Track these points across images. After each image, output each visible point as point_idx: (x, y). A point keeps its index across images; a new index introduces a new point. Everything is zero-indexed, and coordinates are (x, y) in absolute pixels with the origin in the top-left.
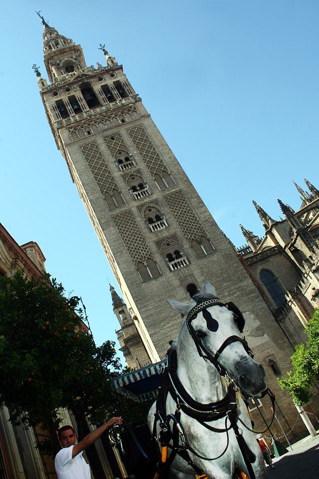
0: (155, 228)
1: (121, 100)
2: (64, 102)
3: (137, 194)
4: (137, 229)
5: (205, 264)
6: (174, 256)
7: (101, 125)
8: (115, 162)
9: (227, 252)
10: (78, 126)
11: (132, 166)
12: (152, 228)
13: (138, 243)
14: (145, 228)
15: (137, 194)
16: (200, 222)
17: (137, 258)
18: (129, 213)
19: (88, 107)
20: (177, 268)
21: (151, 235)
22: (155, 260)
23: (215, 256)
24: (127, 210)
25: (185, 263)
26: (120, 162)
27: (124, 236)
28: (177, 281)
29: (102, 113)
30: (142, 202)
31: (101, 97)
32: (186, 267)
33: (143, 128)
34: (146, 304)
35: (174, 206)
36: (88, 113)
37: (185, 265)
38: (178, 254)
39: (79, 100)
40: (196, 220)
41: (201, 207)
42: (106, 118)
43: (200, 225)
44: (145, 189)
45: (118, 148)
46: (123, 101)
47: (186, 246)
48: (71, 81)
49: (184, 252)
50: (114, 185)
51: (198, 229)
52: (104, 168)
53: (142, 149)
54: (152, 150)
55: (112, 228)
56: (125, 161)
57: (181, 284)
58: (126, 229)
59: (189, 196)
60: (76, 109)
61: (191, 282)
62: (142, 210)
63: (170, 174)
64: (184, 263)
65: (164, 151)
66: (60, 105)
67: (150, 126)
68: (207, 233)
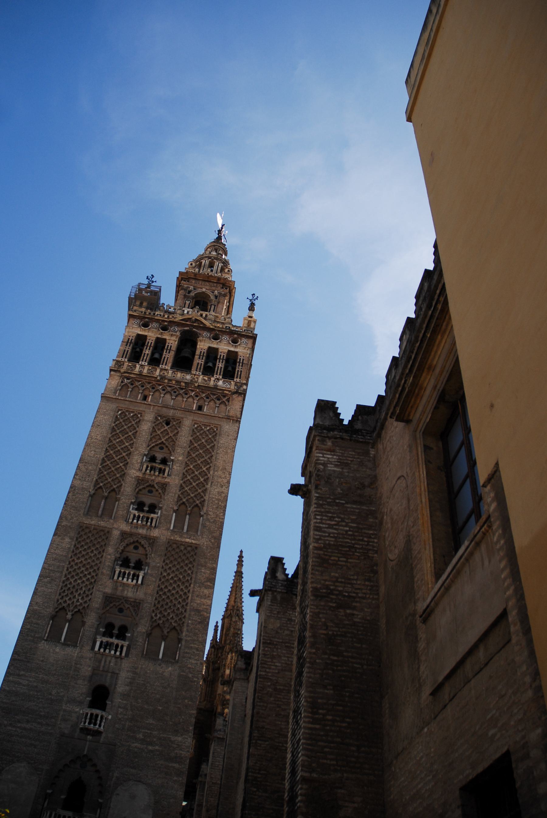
0: (121, 575)
1: (218, 379)
2: (148, 341)
3: (137, 514)
4: (98, 562)
6: (115, 631)
7: (168, 396)
8: (145, 455)
9: (190, 675)
10: (139, 381)
11: (161, 475)
12: (117, 572)
13: (83, 582)
14: (109, 566)
15: (137, 514)
16: (188, 608)
17: (65, 602)
19: (170, 365)
20: (105, 651)
21: (109, 583)
22: (85, 620)
23: (170, 668)
24: (106, 527)
26: (153, 459)
28: (90, 669)
29: (181, 382)
30: (134, 530)
31: (198, 361)
32: (116, 658)
33: (217, 432)
34: (22, 673)
35: (171, 562)
36: (163, 372)
37: (118, 653)
38: (121, 636)
39: (167, 349)
40: (184, 600)
41: (207, 587)
42: (181, 392)
43: (185, 611)
44: (152, 515)
45: (163, 440)
46: (220, 383)
47: (143, 628)
48: (176, 320)
49: (132, 635)
50: (118, 485)
51: (177, 615)
52: (124, 454)
53: (193, 460)
54: (204, 469)
55: (67, 540)
56: (157, 461)
57: (91, 677)
58: (84, 553)
59: (202, 561)
60: (156, 359)
61: (107, 684)
63: (202, 516)
64: (119, 649)
65: (220, 480)
66: (140, 340)
67: (228, 436)
68: (185, 629)
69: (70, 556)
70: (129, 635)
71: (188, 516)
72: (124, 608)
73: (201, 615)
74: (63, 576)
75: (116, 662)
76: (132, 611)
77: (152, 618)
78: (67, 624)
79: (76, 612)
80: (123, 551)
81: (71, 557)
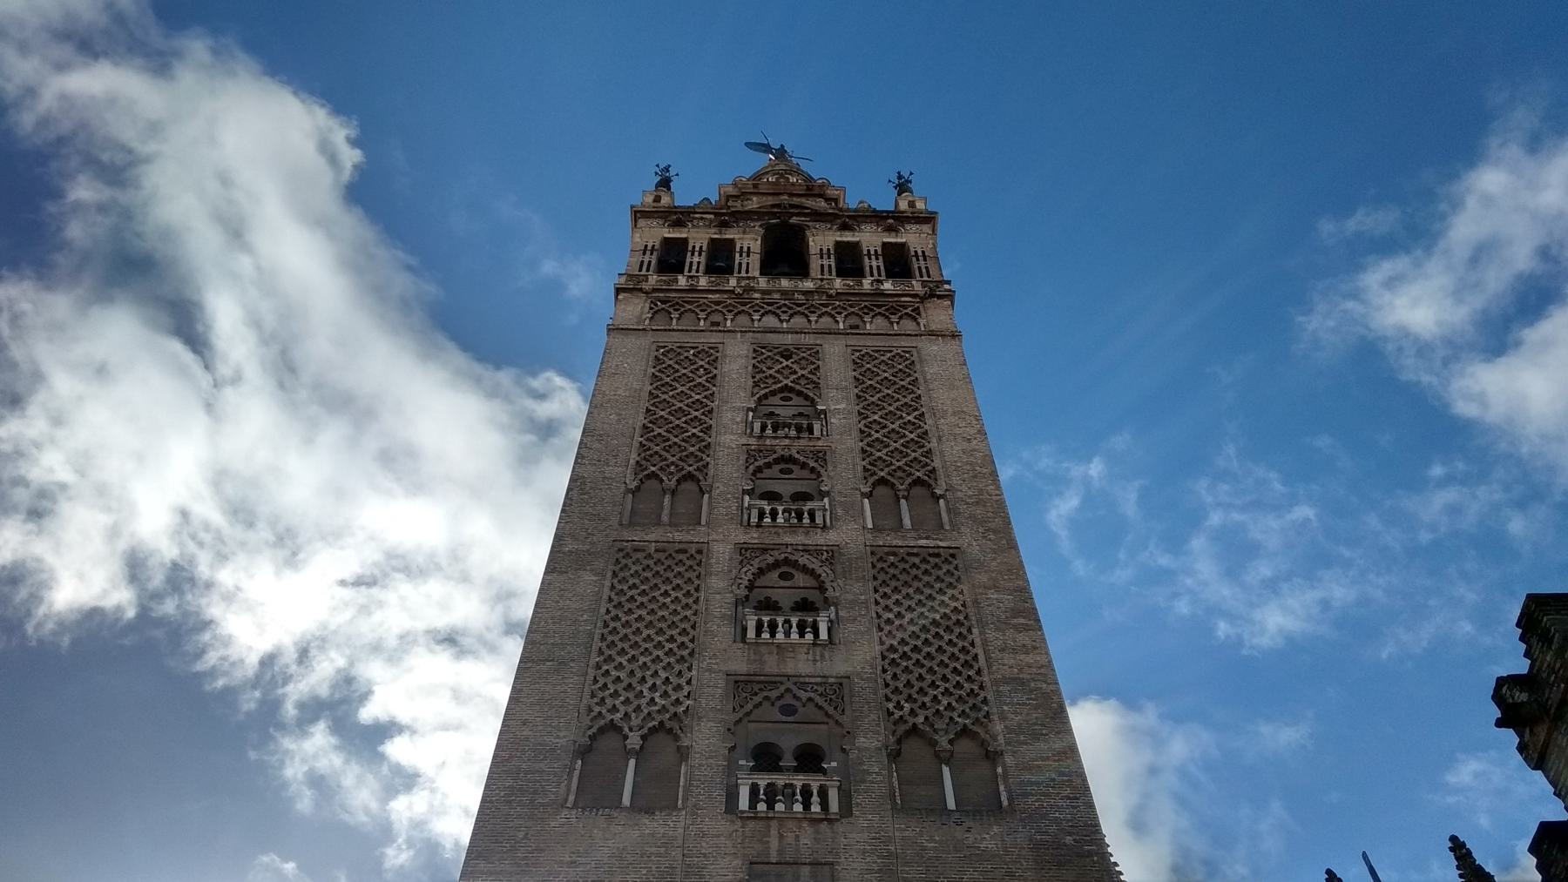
3: (768, 509)
5: (924, 849)
6: (788, 761)
8: (749, 409)
12: (751, 625)
14: (723, 617)
15: (768, 509)
18: (697, 556)
20: (771, 807)
23: (996, 829)
25: (824, 804)
27: (616, 618)
37: (815, 808)
46: (888, 286)
47: (870, 739)
62: (756, 563)
64: (815, 799)
69: (603, 610)
70: (834, 764)
71: (903, 501)
72: (797, 704)
73: (1031, 691)
74: (594, 654)
75: (817, 832)
76: (825, 705)
77: (890, 714)
78: (632, 762)
79: (653, 730)
80: (751, 587)
81: (608, 612)
